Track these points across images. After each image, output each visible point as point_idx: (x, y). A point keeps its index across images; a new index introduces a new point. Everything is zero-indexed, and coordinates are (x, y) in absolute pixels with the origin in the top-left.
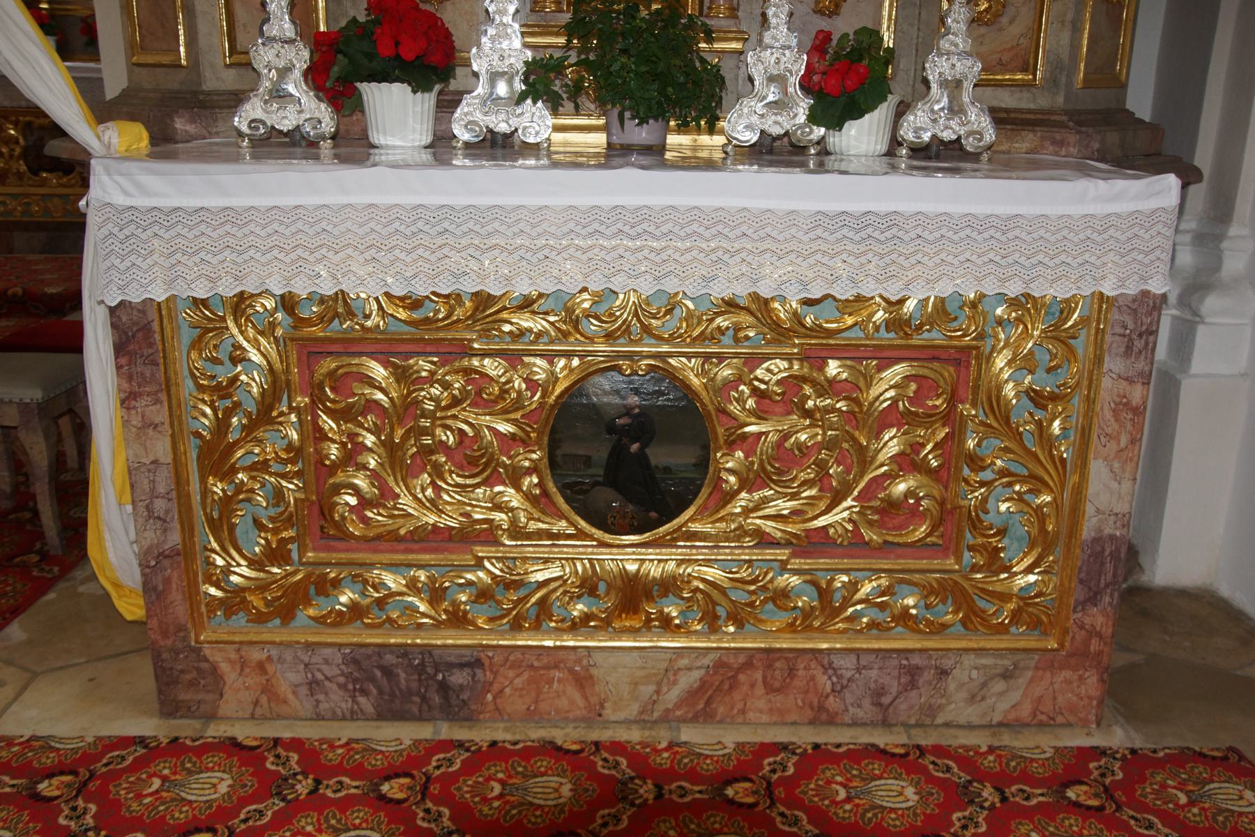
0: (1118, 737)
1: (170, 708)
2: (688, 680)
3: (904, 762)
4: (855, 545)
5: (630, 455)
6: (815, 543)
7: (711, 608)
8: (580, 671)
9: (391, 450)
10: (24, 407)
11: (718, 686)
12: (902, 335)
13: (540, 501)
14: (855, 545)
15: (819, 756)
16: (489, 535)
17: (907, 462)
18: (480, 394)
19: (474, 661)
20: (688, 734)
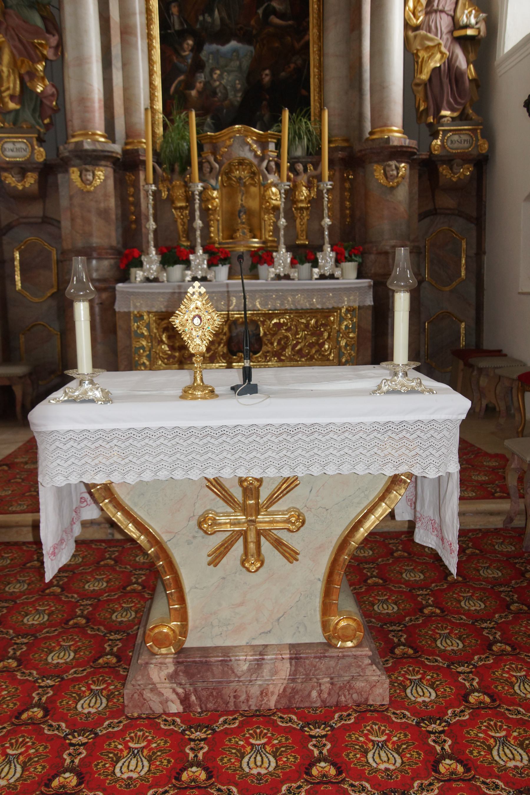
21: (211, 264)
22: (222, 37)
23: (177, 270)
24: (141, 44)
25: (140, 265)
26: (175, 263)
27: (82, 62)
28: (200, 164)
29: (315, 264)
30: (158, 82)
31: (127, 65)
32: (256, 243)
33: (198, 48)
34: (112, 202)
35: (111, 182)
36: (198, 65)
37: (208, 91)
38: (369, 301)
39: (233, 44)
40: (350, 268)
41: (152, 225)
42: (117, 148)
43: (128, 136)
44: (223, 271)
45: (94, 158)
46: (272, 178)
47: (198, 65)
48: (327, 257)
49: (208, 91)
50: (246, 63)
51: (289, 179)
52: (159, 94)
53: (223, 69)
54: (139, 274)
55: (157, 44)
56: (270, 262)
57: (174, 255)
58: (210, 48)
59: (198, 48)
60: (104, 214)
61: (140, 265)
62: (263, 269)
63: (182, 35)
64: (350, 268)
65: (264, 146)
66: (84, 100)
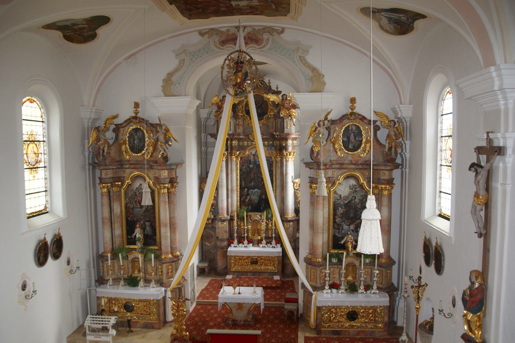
0: (389, 337)
1: (318, 334)
2: (356, 332)
3: (372, 338)
4: (368, 322)
5: (352, 315)
6: (366, 322)
7: (358, 327)
8: (348, 332)
9: (335, 316)
10: (295, 309)
11: (359, 333)
12: (371, 308)
13: (346, 319)
14: (368, 322)
15: (366, 338)
16: (342, 322)
17: (372, 317)
18: (342, 312)
19: (341, 331)
20: (357, 336)
21: (248, 243)
22: (254, 188)
23: (241, 245)
24: (235, 193)
25: (233, 243)
26: (241, 243)
27: (222, 200)
28: (247, 220)
29: (271, 244)
30: (238, 198)
31: (232, 197)
32: (259, 238)
33: (248, 191)
34: (228, 229)
35: (227, 225)
36: (248, 194)
37: (250, 200)
38: (281, 255)
39: (256, 190)
40: (279, 245)
41: (236, 235)
42: (229, 217)
43: (232, 212)
44: (251, 245)
45: (224, 221)
46: (263, 223)
47: (248, 194)
48: (274, 242)
49: (250, 200)
50: (259, 194)
51: (266, 223)
52: (239, 201)
53: (254, 195)
54: (232, 245)
55: (239, 190)
56: (261, 243)
57: (240, 241)
58: (251, 190)
59: (248, 191)
60: (226, 232)
61: (233, 243)
62: (260, 244)
63: (245, 188)
64: (279, 245)
65: (261, 216)
66: (222, 208)
